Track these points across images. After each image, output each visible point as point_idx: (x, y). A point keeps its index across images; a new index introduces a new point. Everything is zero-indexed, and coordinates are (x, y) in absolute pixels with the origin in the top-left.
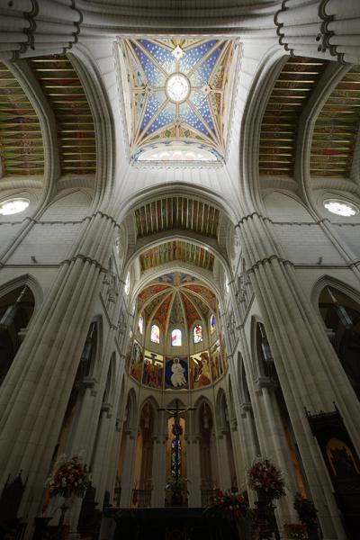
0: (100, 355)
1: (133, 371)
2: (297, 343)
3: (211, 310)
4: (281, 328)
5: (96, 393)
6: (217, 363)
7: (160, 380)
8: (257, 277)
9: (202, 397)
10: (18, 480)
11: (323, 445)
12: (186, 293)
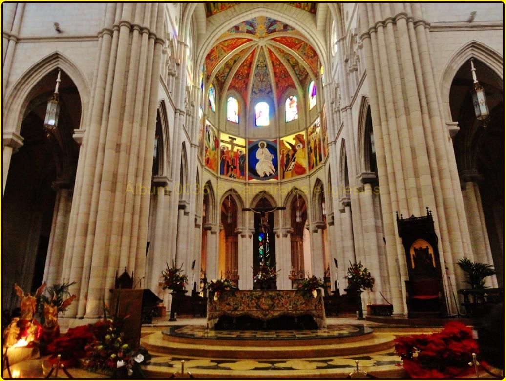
0: (168, 149)
1: (207, 161)
2: (406, 143)
3: (311, 75)
4: (392, 121)
5: (170, 192)
6: (315, 148)
8: (374, 48)
10: (126, 274)
11: (407, 245)
12: (274, 47)
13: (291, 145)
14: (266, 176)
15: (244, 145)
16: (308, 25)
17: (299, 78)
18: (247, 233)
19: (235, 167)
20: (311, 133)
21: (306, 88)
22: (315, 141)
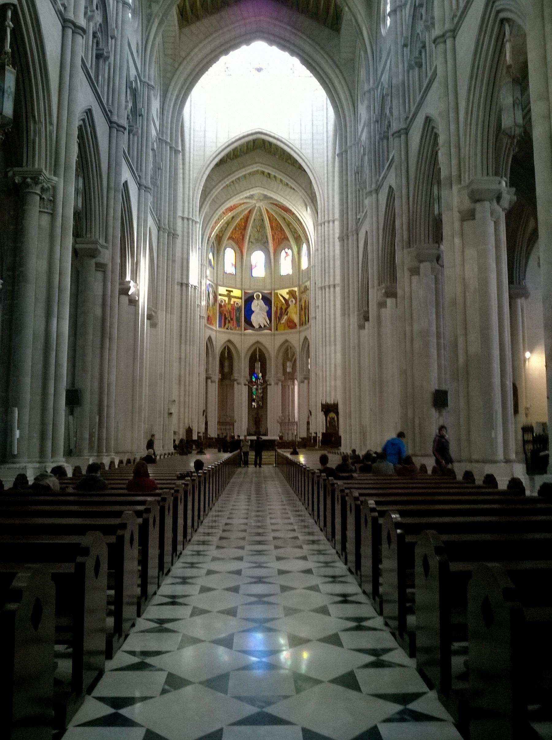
7: (238, 320)
9: (286, 341)
13: (284, 298)
14: (260, 327)
15: (240, 296)
16: (300, 207)
17: (294, 236)
18: (243, 381)
19: (232, 319)
20: (302, 292)
21: (300, 245)
22: (305, 301)
